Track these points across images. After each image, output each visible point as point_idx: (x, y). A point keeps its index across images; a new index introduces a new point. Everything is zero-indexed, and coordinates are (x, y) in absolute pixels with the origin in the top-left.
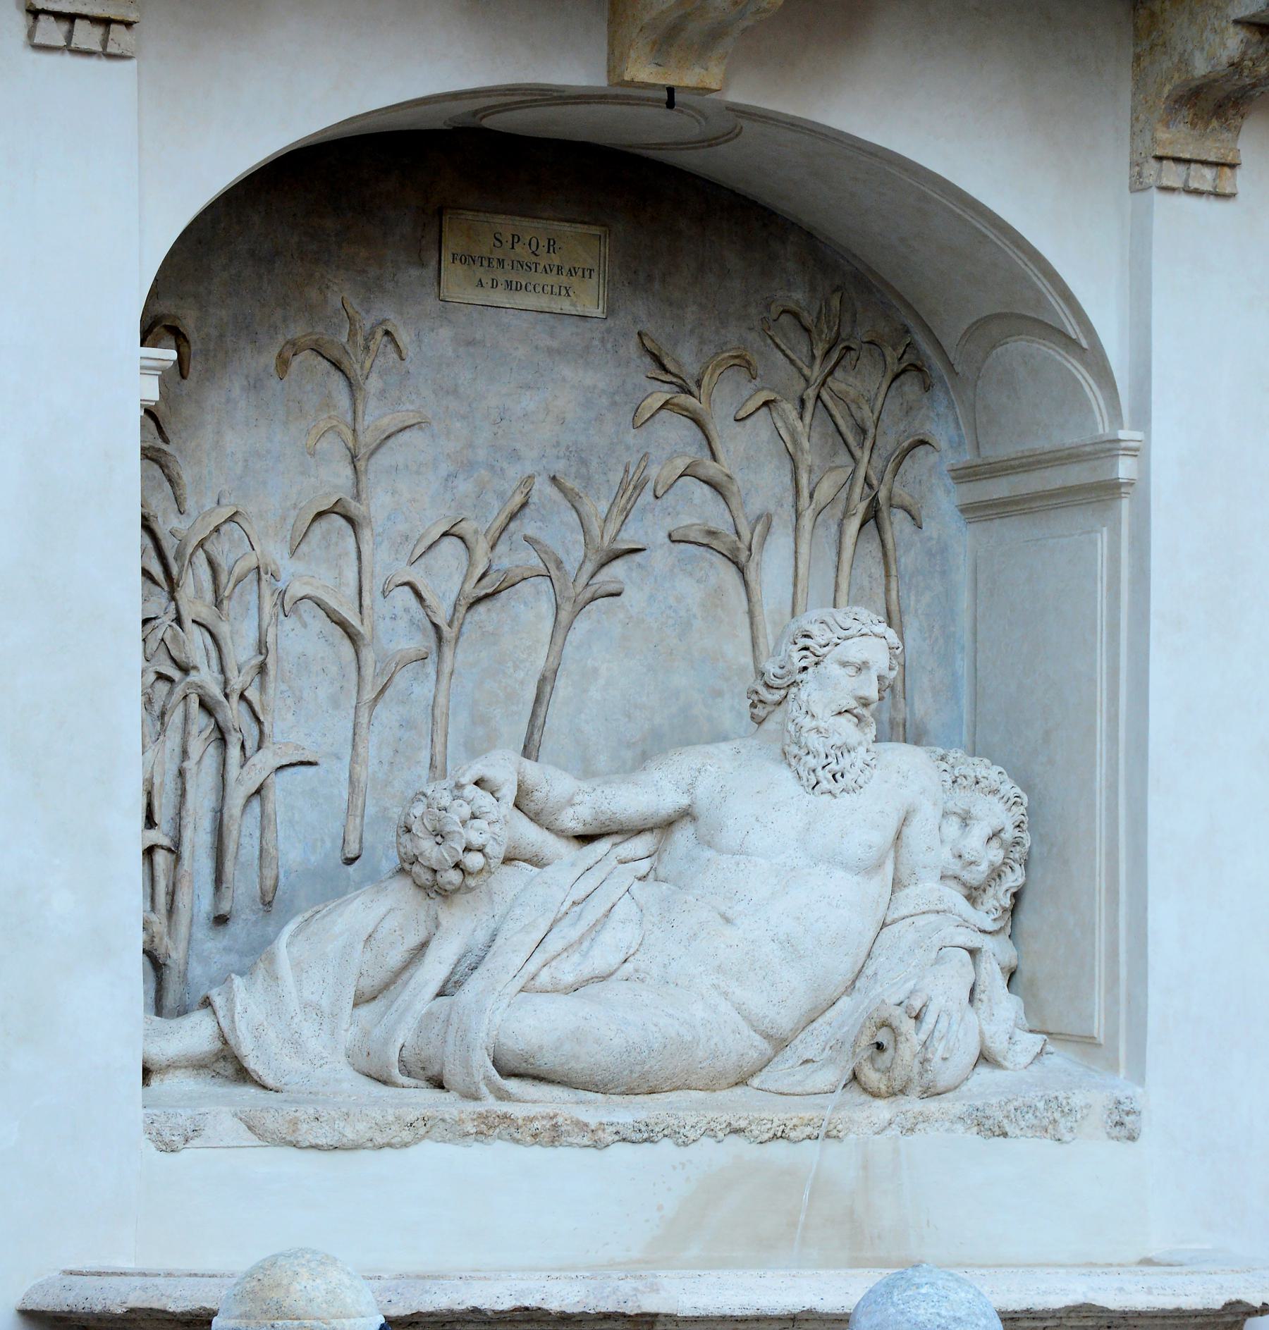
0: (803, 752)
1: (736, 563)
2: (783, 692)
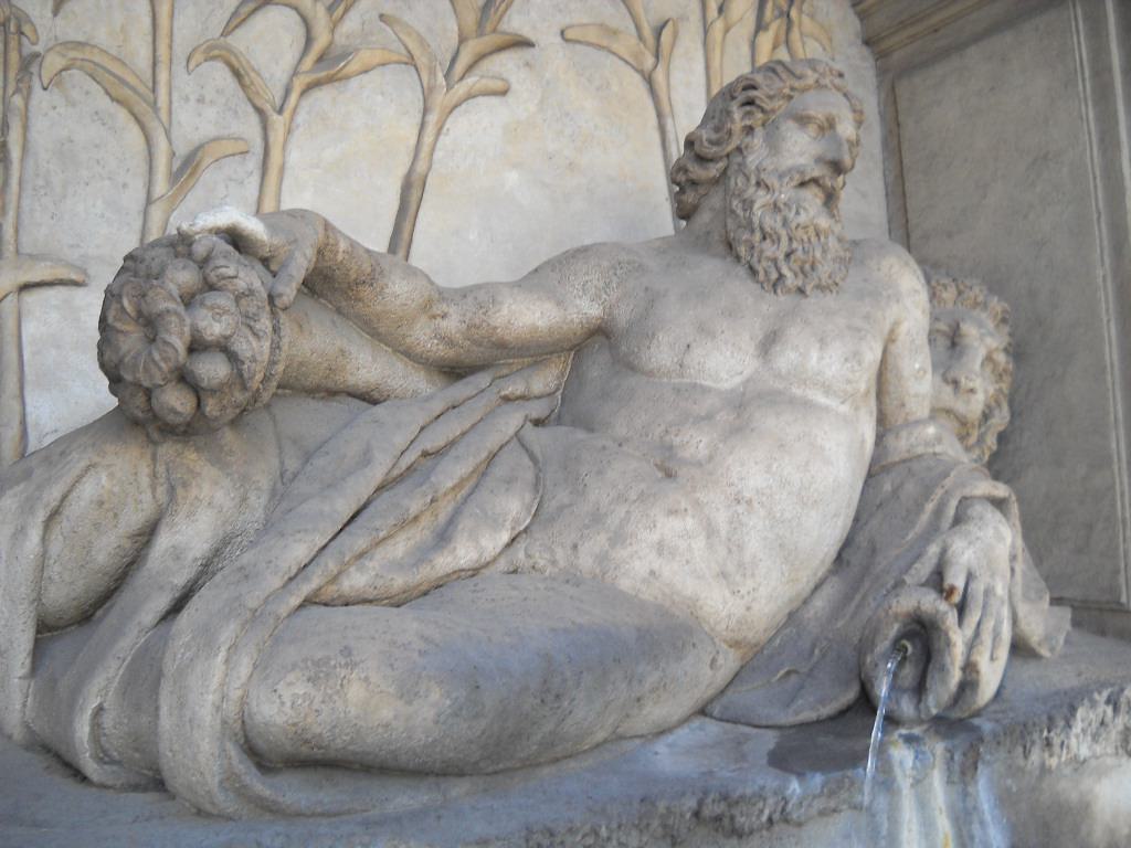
0: (758, 236)
1: (641, 72)
2: (721, 165)
